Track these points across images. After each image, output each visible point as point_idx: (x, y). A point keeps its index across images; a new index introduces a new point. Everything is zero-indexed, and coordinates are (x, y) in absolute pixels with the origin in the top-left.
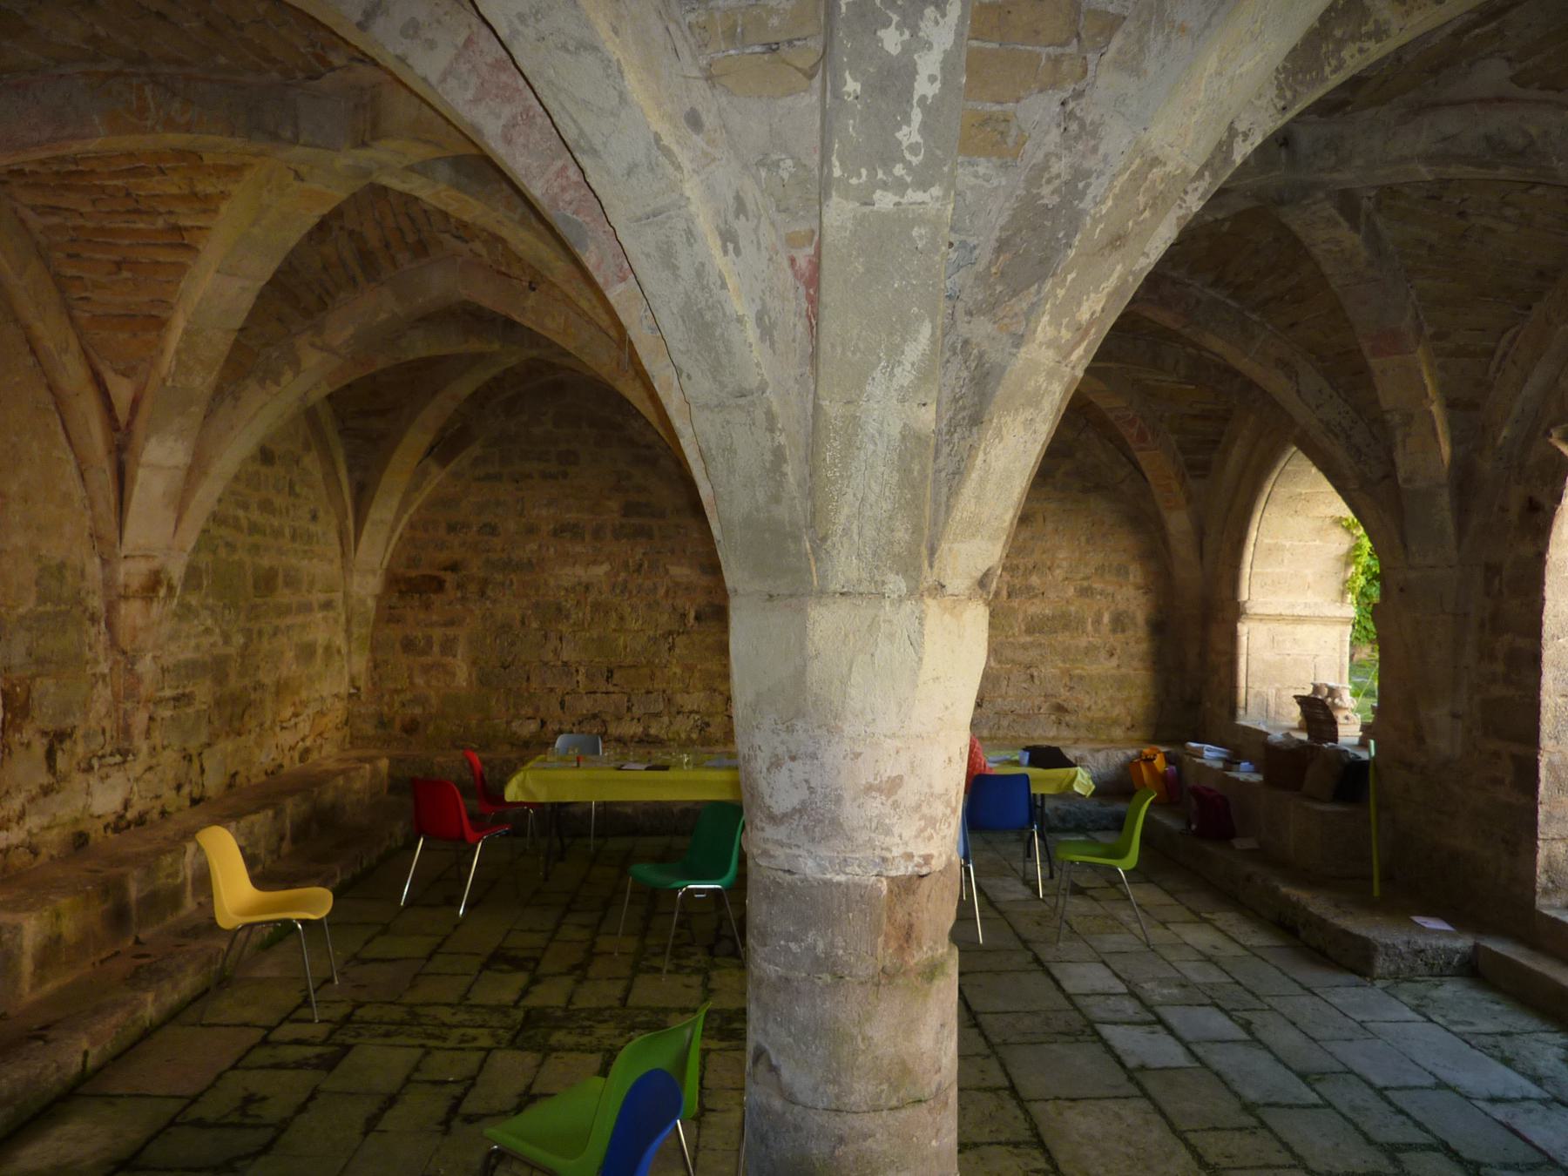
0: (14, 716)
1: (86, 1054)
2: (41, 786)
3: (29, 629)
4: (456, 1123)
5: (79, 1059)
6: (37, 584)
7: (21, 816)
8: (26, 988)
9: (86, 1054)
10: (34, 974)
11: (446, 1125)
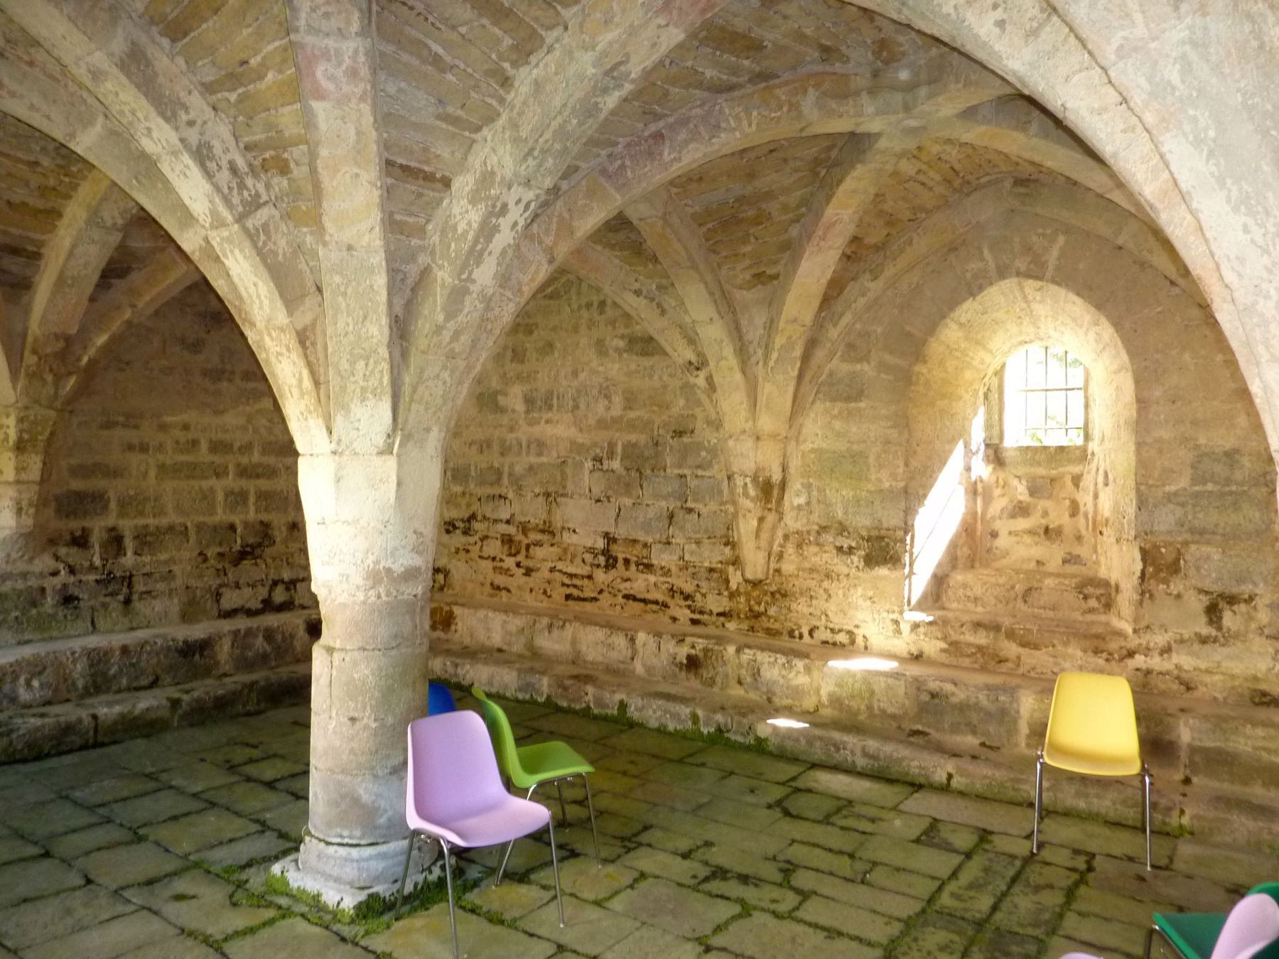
0: (1158, 570)
1: (950, 776)
2: (1198, 635)
3: (1183, 505)
5: (944, 776)
6: (1193, 467)
7: (1166, 650)
8: (1023, 743)
9: (950, 776)
10: (1029, 737)
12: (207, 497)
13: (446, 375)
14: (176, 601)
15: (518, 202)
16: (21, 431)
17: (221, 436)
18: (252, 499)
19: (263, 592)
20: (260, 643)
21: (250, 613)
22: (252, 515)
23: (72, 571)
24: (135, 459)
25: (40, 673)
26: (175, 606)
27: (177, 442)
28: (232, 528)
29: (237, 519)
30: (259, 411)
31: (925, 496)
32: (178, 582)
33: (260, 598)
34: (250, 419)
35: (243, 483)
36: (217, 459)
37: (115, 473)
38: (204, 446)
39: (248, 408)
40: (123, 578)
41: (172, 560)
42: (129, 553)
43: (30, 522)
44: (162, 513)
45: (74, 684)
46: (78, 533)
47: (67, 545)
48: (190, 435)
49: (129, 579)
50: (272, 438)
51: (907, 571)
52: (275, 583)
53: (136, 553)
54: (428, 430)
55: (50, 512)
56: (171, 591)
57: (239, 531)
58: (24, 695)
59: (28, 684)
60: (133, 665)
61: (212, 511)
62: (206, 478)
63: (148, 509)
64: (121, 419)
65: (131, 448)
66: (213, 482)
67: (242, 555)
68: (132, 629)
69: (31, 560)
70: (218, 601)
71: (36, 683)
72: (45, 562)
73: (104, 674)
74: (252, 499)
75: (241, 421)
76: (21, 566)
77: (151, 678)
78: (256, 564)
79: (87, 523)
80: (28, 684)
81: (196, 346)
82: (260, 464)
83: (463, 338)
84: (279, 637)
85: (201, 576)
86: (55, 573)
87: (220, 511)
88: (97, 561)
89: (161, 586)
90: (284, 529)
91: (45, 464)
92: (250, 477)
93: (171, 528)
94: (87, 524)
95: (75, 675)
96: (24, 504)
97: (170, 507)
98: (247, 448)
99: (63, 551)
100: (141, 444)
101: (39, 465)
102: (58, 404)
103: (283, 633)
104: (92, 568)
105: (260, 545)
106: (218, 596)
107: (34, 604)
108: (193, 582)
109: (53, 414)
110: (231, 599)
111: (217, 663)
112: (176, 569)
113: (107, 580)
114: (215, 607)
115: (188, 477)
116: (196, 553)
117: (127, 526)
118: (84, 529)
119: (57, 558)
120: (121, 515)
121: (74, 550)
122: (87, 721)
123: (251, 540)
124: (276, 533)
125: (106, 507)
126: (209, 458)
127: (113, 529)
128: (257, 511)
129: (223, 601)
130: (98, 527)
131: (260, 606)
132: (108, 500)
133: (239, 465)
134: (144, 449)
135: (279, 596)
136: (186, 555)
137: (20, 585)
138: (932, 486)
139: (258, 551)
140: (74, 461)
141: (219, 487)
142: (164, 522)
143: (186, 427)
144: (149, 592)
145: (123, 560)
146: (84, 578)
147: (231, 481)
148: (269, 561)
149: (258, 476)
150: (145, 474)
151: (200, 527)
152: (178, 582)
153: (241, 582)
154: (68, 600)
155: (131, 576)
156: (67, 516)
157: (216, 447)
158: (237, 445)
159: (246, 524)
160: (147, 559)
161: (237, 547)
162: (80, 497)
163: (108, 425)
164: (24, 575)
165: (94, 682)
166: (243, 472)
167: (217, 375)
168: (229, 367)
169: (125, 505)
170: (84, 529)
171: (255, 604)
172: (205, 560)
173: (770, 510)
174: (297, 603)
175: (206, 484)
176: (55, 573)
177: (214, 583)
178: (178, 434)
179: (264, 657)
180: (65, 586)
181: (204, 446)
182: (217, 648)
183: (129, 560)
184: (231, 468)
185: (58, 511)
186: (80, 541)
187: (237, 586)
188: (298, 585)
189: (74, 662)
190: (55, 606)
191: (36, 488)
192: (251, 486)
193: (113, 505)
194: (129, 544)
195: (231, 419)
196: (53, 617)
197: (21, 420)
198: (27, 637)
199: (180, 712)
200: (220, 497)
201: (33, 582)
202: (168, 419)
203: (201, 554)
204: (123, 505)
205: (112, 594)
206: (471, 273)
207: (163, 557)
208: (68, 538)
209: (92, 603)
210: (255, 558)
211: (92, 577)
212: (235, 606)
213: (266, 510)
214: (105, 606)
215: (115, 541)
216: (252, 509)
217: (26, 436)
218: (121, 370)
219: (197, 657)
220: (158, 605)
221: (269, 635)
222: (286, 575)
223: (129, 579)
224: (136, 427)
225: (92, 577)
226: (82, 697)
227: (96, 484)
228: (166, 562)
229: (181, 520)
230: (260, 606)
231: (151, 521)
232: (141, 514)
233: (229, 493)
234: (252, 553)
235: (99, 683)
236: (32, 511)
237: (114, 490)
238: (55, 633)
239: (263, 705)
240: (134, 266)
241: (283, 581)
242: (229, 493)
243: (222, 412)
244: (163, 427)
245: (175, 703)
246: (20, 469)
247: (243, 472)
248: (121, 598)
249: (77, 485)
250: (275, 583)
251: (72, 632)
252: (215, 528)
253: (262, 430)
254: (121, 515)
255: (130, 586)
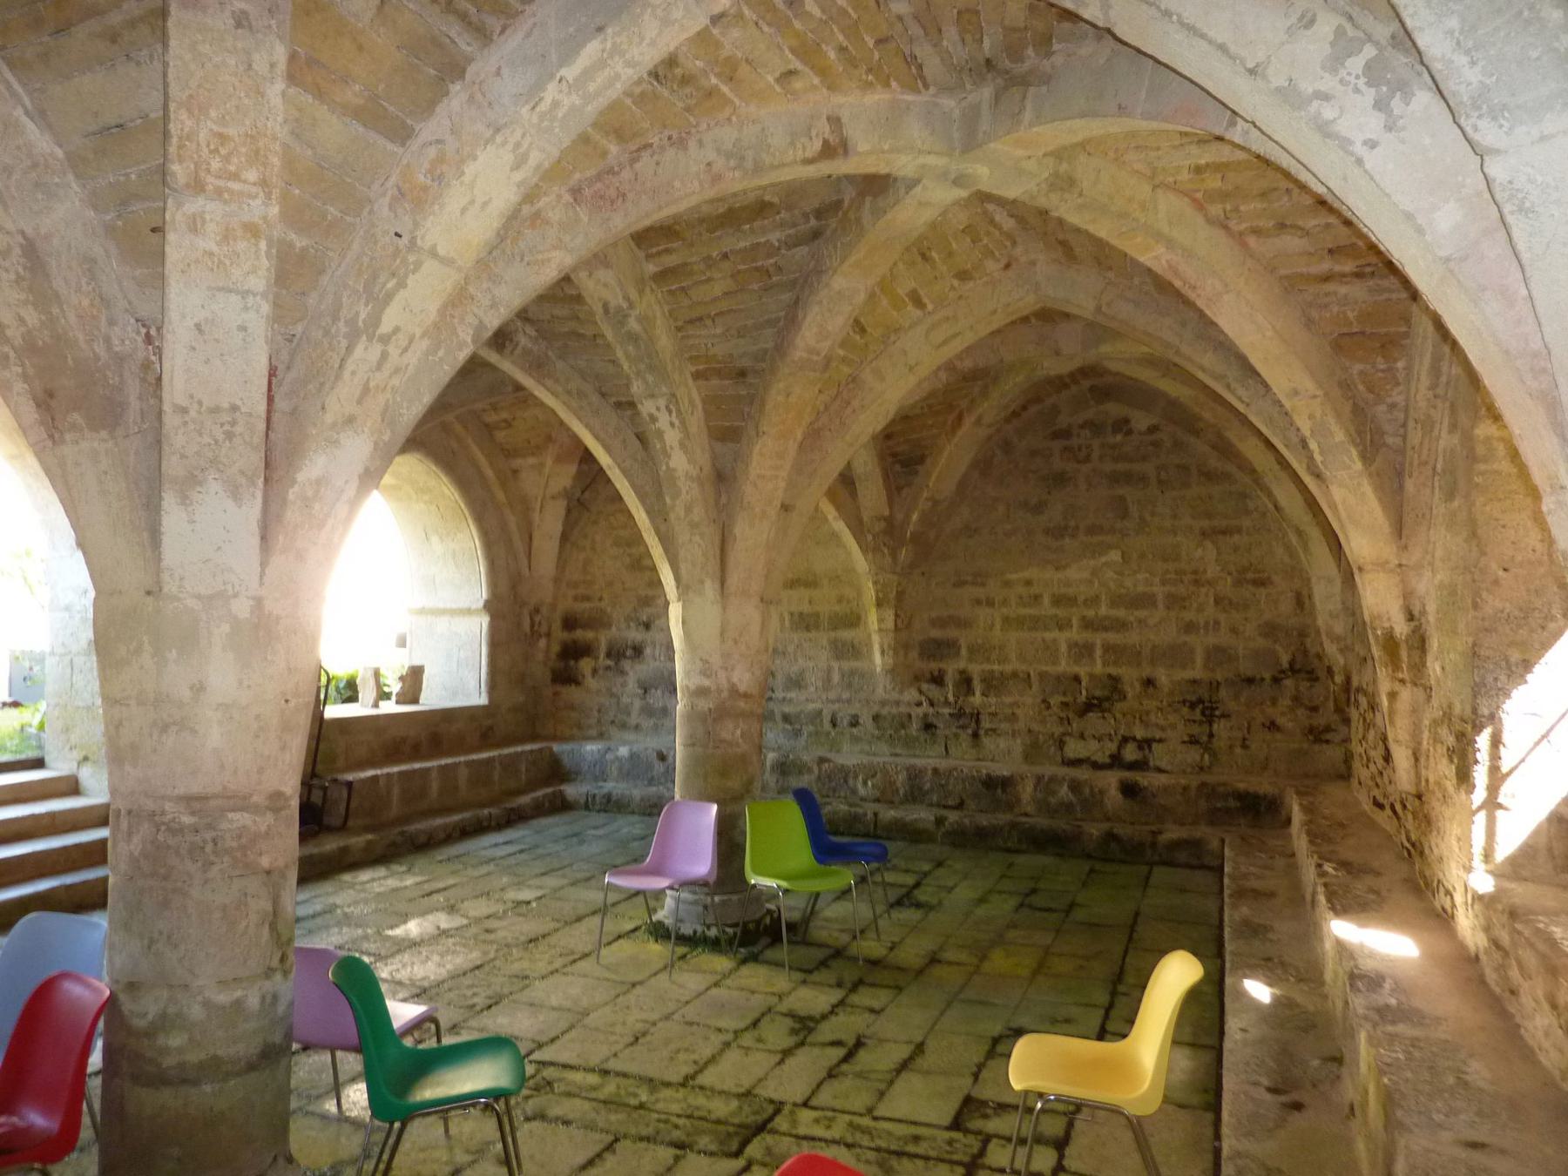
4: (851, 1042)
11: (859, 1044)
12: (1050, 649)
13: (697, 538)
14: (1019, 741)
15: (658, 409)
16: (877, 592)
17: (1063, 590)
18: (1098, 652)
19: (1112, 747)
20: (1064, 792)
21: (1097, 766)
22: (1098, 668)
23: (932, 704)
24: (983, 614)
25: (874, 776)
26: (1018, 746)
27: (1021, 598)
28: (1077, 679)
29: (1082, 671)
30: (1106, 564)
31: (1528, 665)
32: (1021, 725)
33: (1107, 753)
34: (1095, 572)
35: (1088, 636)
36: (1061, 612)
37: (963, 624)
38: (1046, 600)
39: (1092, 562)
40: (972, 714)
41: (1016, 704)
42: (978, 693)
43: (891, 661)
44: (1003, 660)
45: (897, 790)
46: (936, 673)
47: (928, 681)
48: (1035, 590)
49: (977, 717)
50: (1123, 591)
51: (1479, 795)
52: (1125, 740)
53: (983, 694)
54: (702, 582)
55: (914, 654)
56: (1014, 731)
57: (1084, 684)
58: (862, 791)
59: (865, 783)
60: (942, 786)
61: (1055, 662)
62: (1046, 628)
63: (994, 657)
64: (969, 578)
65: (978, 602)
66: (1055, 634)
67: (1089, 707)
68: (979, 760)
69: (901, 692)
70: (1061, 749)
71: (870, 783)
72: (911, 695)
73: (920, 789)
74: (1098, 652)
75: (1086, 575)
76: (895, 696)
77: (958, 801)
78: (1104, 718)
79: (943, 665)
80: (865, 783)
81: (1038, 508)
82: (1106, 618)
83: (696, 510)
84: (1087, 791)
85: (1043, 722)
86: (919, 704)
87: (1063, 663)
88: (951, 698)
89: (1004, 726)
90: (1137, 685)
91: (897, 615)
92: (1097, 630)
93: (1015, 675)
94: (943, 665)
95: (899, 784)
96: (886, 647)
97: (1013, 656)
98: (1094, 601)
99: (925, 686)
100: (988, 599)
101: (892, 617)
102: (898, 569)
103: (1092, 788)
104: (947, 703)
105: (1108, 699)
106: (1061, 744)
107: (903, 726)
108: (1036, 727)
109: (895, 578)
110: (1074, 749)
111: (1019, 801)
112: (1018, 711)
113: (959, 715)
114: (1059, 753)
115: (1030, 629)
116: (1039, 700)
117: (975, 670)
118: (940, 671)
119: (921, 692)
120: (970, 660)
121: (933, 687)
122: (870, 816)
123: (1098, 693)
124: (1127, 688)
125: (958, 654)
126: (1053, 611)
127: (962, 672)
128: (1104, 665)
129: (1066, 749)
130: (951, 668)
131: (1108, 760)
132: (960, 647)
133: (1083, 618)
134: (990, 603)
135: (1130, 753)
136: (1029, 700)
137: (894, 711)
138: (1546, 646)
139: (1106, 705)
140: (934, 615)
141: (1062, 638)
142: (1008, 668)
143: (1028, 583)
144: (994, 730)
145: (971, 699)
146: (940, 711)
147: (1074, 634)
148: (1118, 716)
149: (1106, 629)
150: (992, 626)
151: (1043, 676)
152: (1021, 725)
153: (1086, 734)
154: (928, 727)
155: (978, 714)
156: (929, 657)
157: (1058, 601)
158: (1081, 598)
159: (1092, 676)
160: (993, 700)
161: (1083, 698)
162: (938, 644)
163: (960, 584)
164: (898, 703)
165: (912, 793)
166: (1088, 624)
167: (1058, 532)
168: (1072, 523)
169: (973, 650)
170: (940, 671)
171: (1102, 758)
172: (1049, 707)
173: (1402, 681)
174: (1151, 764)
175: (1049, 636)
176: (919, 704)
177: (1058, 730)
178: (1021, 590)
179: (1068, 807)
180: (926, 715)
181: (1046, 600)
182: (1020, 788)
183: (977, 699)
184: (1075, 621)
185: (921, 655)
186: (938, 680)
187: (1082, 736)
188: (1154, 745)
189: (897, 773)
190: (918, 730)
191: (892, 635)
192: (1098, 639)
193: (964, 652)
194: (978, 687)
195: (1073, 573)
196: (917, 739)
197: (875, 583)
198: (898, 751)
199: (943, 830)
200: (1063, 648)
201: (903, 709)
202: (1014, 576)
203: (1044, 701)
204: (973, 650)
205: (963, 727)
206: (667, 464)
207: (1008, 700)
208: (928, 676)
209: (947, 732)
210: (1103, 711)
211: (946, 711)
212: (1081, 756)
213: (1115, 663)
214: (956, 736)
215: (965, 682)
216: (1099, 662)
217: (881, 595)
218: (970, 537)
219: (999, 791)
220: (1003, 743)
221: (1075, 786)
222: (1140, 733)
223: (977, 717)
224: (983, 585)
225: (946, 711)
226: (902, 803)
227: (951, 633)
228: (1012, 705)
229: (1024, 667)
230: (1108, 760)
231: (996, 667)
232: (988, 660)
233: (1072, 645)
234: (1099, 706)
235: (915, 794)
236: (891, 653)
237: (964, 639)
238: (917, 753)
239: (1024, 846)
240: (927, 452)
241: (1134, 739)
242: (1072, 645)
243: (1065, 567)
244: (1007, 584)
245: (940, 821)
246: (881, 620)
247: (1088, 624)
248: (970, 731)
249: (936, 633)
250: (1125, 740)
251: (931, 753)
252: (1058, 678)
253: (1112, 585)
254: (970, 660)
255: (978, 721)
